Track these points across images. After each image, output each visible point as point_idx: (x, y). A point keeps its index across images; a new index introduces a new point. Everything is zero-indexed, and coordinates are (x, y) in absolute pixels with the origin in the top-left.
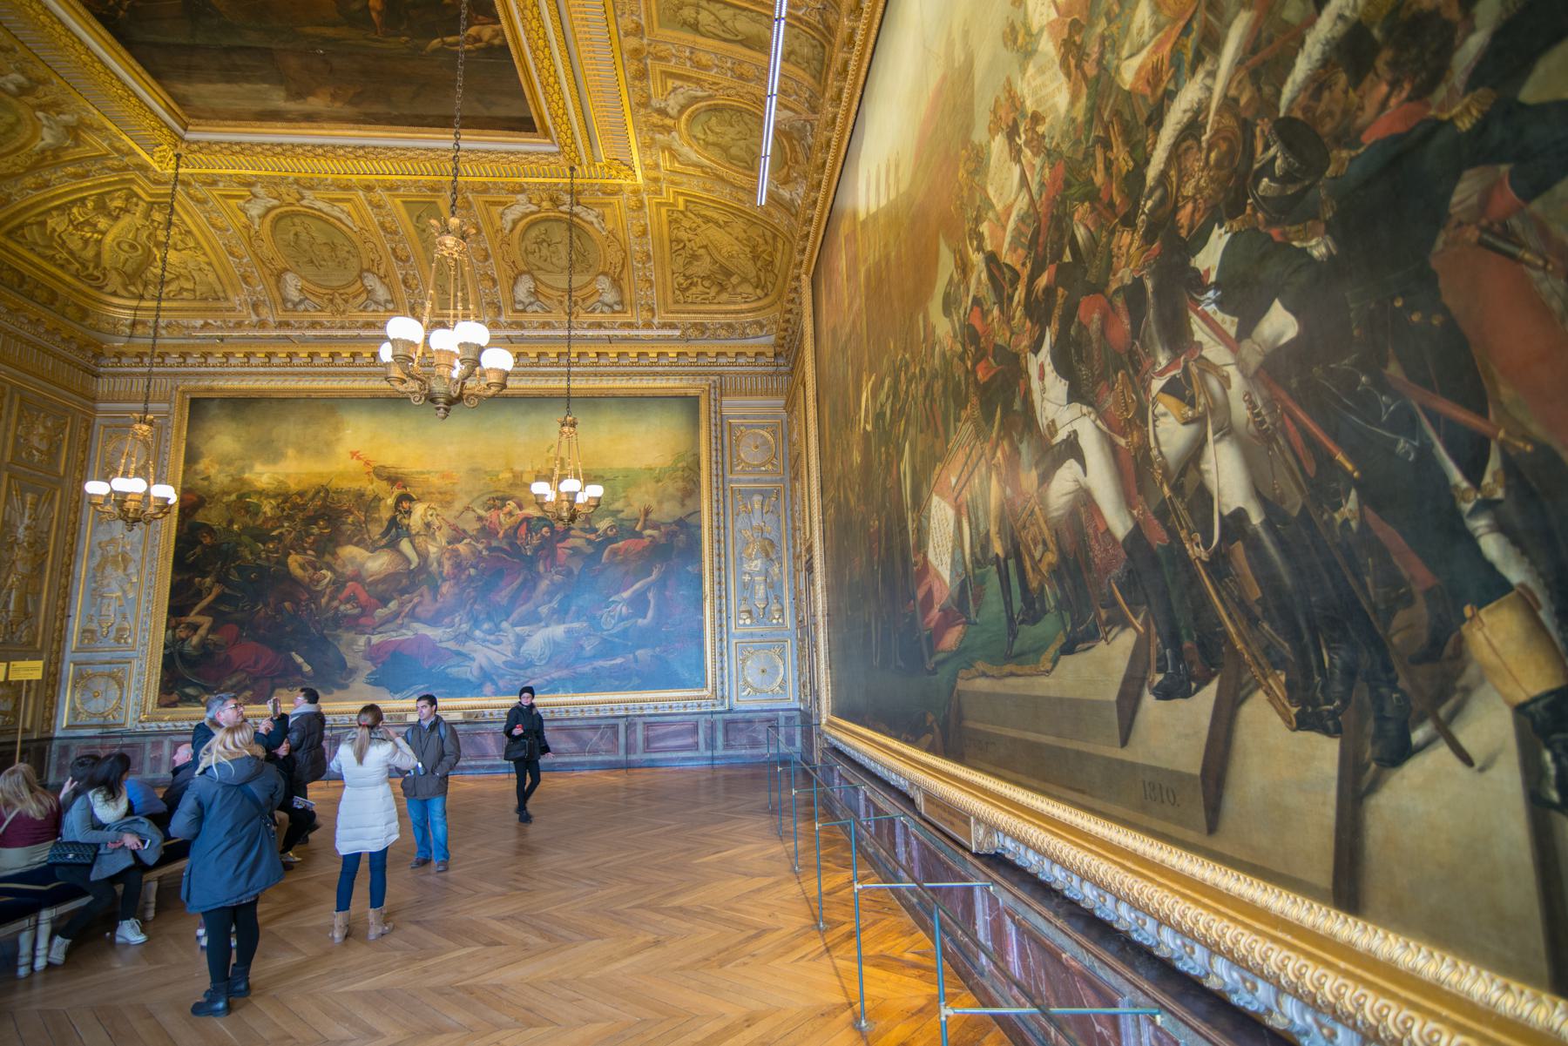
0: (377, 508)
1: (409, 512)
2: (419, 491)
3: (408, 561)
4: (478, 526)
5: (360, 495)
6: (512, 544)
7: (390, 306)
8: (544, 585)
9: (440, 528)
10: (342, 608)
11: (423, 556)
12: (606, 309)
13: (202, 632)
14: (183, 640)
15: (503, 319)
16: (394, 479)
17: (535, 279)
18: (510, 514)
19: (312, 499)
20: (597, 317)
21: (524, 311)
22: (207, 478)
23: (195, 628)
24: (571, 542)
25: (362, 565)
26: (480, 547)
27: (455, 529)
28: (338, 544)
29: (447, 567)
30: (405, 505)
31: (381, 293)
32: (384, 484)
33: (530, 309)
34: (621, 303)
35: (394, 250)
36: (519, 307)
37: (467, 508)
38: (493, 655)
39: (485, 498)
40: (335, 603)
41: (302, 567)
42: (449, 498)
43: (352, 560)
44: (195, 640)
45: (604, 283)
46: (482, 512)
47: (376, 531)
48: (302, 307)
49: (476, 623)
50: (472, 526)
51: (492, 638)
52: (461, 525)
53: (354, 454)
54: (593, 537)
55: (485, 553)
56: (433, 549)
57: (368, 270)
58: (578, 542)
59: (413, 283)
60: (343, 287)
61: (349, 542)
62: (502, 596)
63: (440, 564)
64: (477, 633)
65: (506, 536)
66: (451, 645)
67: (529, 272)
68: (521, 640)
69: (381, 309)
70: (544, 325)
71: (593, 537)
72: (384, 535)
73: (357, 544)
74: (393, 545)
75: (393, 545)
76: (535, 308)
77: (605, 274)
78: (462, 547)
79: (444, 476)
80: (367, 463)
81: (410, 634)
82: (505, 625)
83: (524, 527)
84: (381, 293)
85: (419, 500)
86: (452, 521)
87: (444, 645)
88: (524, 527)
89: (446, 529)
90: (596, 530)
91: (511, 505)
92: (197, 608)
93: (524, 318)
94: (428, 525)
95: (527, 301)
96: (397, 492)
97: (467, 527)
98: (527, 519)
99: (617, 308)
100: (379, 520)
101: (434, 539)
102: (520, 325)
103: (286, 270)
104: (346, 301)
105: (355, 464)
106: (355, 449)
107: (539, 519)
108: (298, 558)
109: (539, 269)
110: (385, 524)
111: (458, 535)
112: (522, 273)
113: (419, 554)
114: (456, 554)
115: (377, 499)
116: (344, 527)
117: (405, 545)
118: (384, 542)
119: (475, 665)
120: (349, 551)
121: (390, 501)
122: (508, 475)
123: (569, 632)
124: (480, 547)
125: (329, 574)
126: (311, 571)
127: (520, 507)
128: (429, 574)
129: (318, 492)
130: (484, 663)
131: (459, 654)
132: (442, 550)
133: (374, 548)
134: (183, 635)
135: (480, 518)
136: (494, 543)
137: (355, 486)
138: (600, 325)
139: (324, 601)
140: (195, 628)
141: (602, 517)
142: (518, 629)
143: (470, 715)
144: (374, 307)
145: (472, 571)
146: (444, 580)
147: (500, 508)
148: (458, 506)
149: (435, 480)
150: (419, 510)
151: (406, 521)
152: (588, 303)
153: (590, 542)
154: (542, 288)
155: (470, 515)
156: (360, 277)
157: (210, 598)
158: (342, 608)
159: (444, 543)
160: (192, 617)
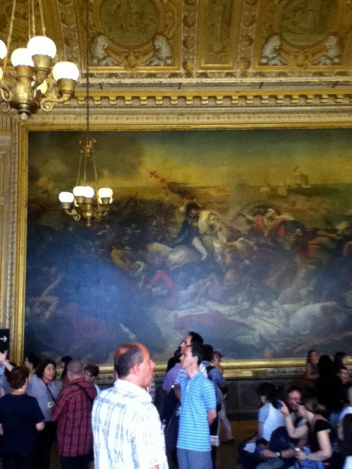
0: (173, 215)
1: (197, 218)
2: (203, 201)
3: (200, 254)
4: (248, 227)
5: (159, 204)
6: (275, 242)
7: (169, 61)
8: (302, 273)
9: (220, 229)
10: (154, 290)
11: (210, 250)
12: (328, 61)
13: (52, 308)
14: (39, 315)
15: (251, 70)
16: (184, 192)
17: (282, 39)
18: (271, 218)
19: (125, 208)
20: (321, 68)
21: (267, 64)
22: (46, 192)
23: (46, 305)
24: (318, 240)
25: (166, 257)
26: (251, 243)
27: (231, 229)
28: (148, 242)
29: (229, 259)
30: (194, 212)
31: (165, 51)
32: (176, 197)
33: (272, 62)
34: (339, 57)
35: (185, 17)
36: (264, 61)
37: (239, 215)
38: (269, 327)
39: (252, 206)
40: (149, 286)
41: (122, 258)
42: (225, 206)
43: (158, 253)
44: (47, 314)
45: (332, 41)
46: (250, 218)
47: (174, 231)
48: (104, 62)
49: (254, 302)
50: (244, 228)
51: (267, 313)
52: (236, 227)
53: (153, 174)
54: (333, 235)
55: (256, 248)
56: (217, 245)
57: (161, 34)
58: (324, 240)
59: (189, 43)
60: (138, 47)
61: (155, 240)
62: (271, 282)
63: (223, 256)
64: (256, 309)
65: (270, 235)
66: (237, 318)
67: (279, 34)
68: (288, 315)
69: (162, 63)
70: (280, 74)
71: (333, 235)
72: (180, 234)
73: (161, 242)
74: (187, 243)
75: (187, 243)
76: (275, 61)
77: (335, 34)
78: (238, 244)
79: (219, 190)
80: (163, 181)
81: (206, 311)
82: (275, 303)
83: (282, 228)
84: (165, 51)
85: (204, 208)
86: (229, 224)
87: (233, 318)
88: (282, 228)
89: (225, 230)
90: (335, 231)
91: (271, 211)
92: (47, 291)
93: (266, 70)
94: (212, 227)
95: (271, 56)
96: (186, 202)
97: (240, 228)
98: (284, 222)
99: (336, 60)
100: (175, 223)
101: (217, 238)
102: (262, 75)
103: (100, 34)
104: (137, 58)
105: (153, 181)
106: (153, 169)
107: (293, 222)
108: (119, 252)
109: (289, 31)
110: (180, 226)
111: (234, 235)
112: (276, 34)
113: (207, 249)
114: (234, 250)
115: (173, 208)
116: (150, 229)
117: (196, 242)
118: (180, 240)
119: (256, 334)
120: (157, 247)
121: (182, 209)
122: (265, 189)
123: (324, 309)
124: (251, 243)
125: (142, 264)
126: (129, 262)
127: (278, 213)
128: (216, 263)
129: (128, 203)
130: (262, 332)
131: (243, 325)
132: (224, 246)
133: (173, 245)
134: (38, 310)
135: (249, 222)
136: (262, 241)
137: (155, 197)
138: (321, 74)
139: (140, 284)
140: (46, 305)
141: (340, 221)
142: (286, 306)
143: (258, 372)
144: (156, 62)
145: (247, 262)
146: (227, 269)
147: (263, 214)
148: (232, 212)
149: (213, 193)
150: (204, 215)
151: (195, 224)
152: (316, 57)
153: (332, 239)
154: (286, 47)
155: (242, 220)
156: (153, 39)
157: (56, 283)
158: (154, 290)
159: (224, 240)
160: (44, 297)
